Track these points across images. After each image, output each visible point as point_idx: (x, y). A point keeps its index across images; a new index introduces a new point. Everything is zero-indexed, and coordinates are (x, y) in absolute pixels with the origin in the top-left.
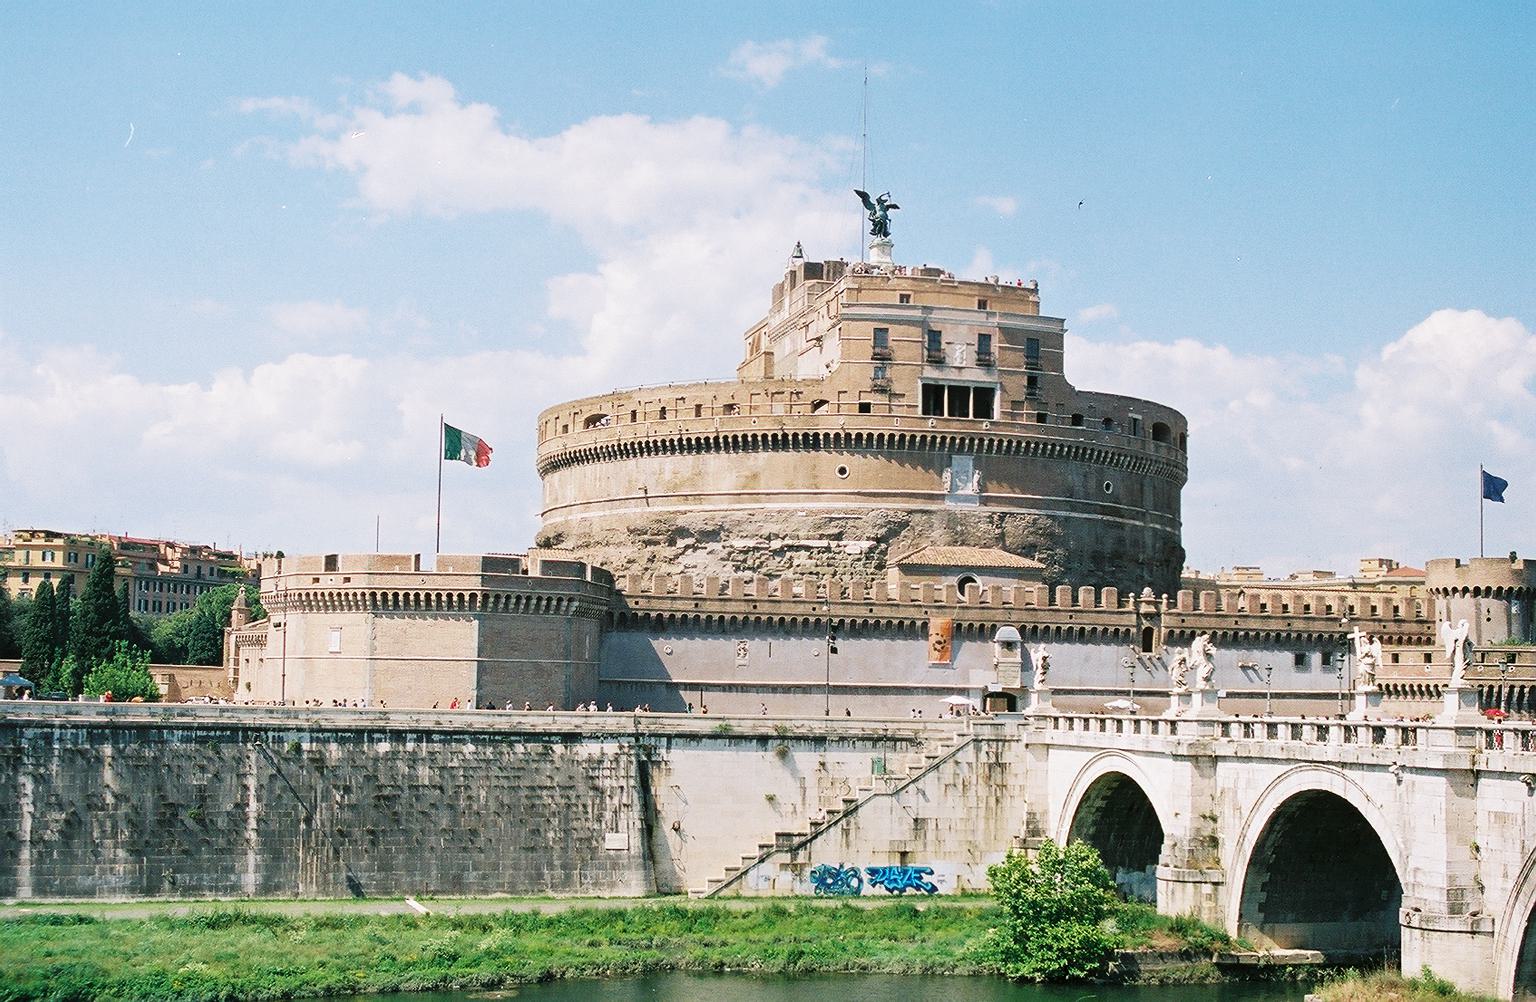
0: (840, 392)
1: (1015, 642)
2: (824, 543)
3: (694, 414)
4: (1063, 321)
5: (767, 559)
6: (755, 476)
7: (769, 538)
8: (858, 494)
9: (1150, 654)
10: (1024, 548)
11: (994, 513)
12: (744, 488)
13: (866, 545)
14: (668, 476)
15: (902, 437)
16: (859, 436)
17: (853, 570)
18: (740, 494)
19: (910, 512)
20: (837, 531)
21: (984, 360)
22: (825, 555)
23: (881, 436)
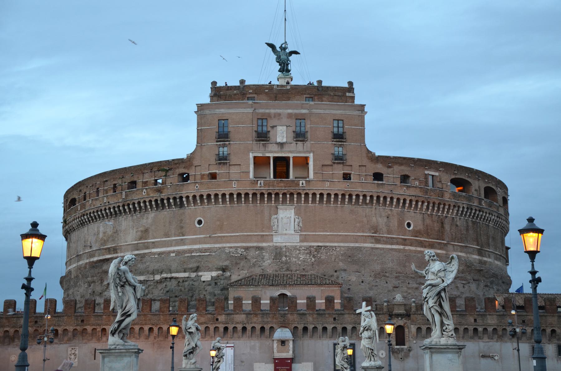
0: (195, 166)
1: (288, 340)
2: (186, 275)
3: (112, 191)
4: (363, 106)
5: (153, 288)
6: (146, 231)
7: (153, 273)
8: (210, 237)
9: (402, 347)
10: (336, 271)
11: (310, 246)
12: (140, 239)
13: (214, 274)
14: (101, 235)
15: (239, 195)
16: (209, 196)
17: (205, 293)
18: (138, 243)
19: (247, 249)
20: (195, 265)
21: (300, 136)
22: (187, 283)
23: (224, 195)
